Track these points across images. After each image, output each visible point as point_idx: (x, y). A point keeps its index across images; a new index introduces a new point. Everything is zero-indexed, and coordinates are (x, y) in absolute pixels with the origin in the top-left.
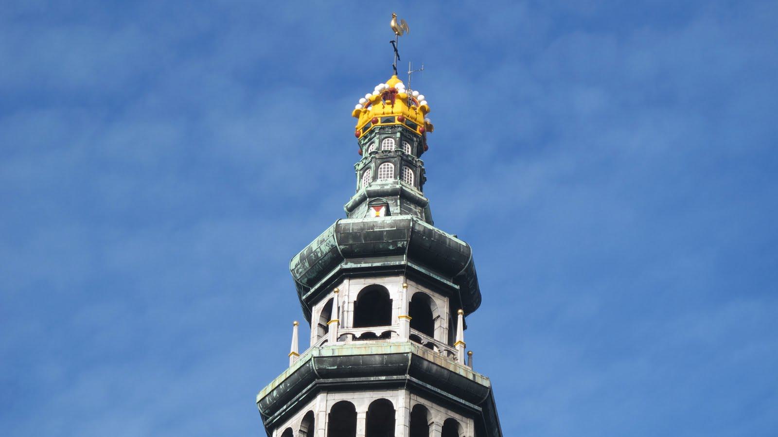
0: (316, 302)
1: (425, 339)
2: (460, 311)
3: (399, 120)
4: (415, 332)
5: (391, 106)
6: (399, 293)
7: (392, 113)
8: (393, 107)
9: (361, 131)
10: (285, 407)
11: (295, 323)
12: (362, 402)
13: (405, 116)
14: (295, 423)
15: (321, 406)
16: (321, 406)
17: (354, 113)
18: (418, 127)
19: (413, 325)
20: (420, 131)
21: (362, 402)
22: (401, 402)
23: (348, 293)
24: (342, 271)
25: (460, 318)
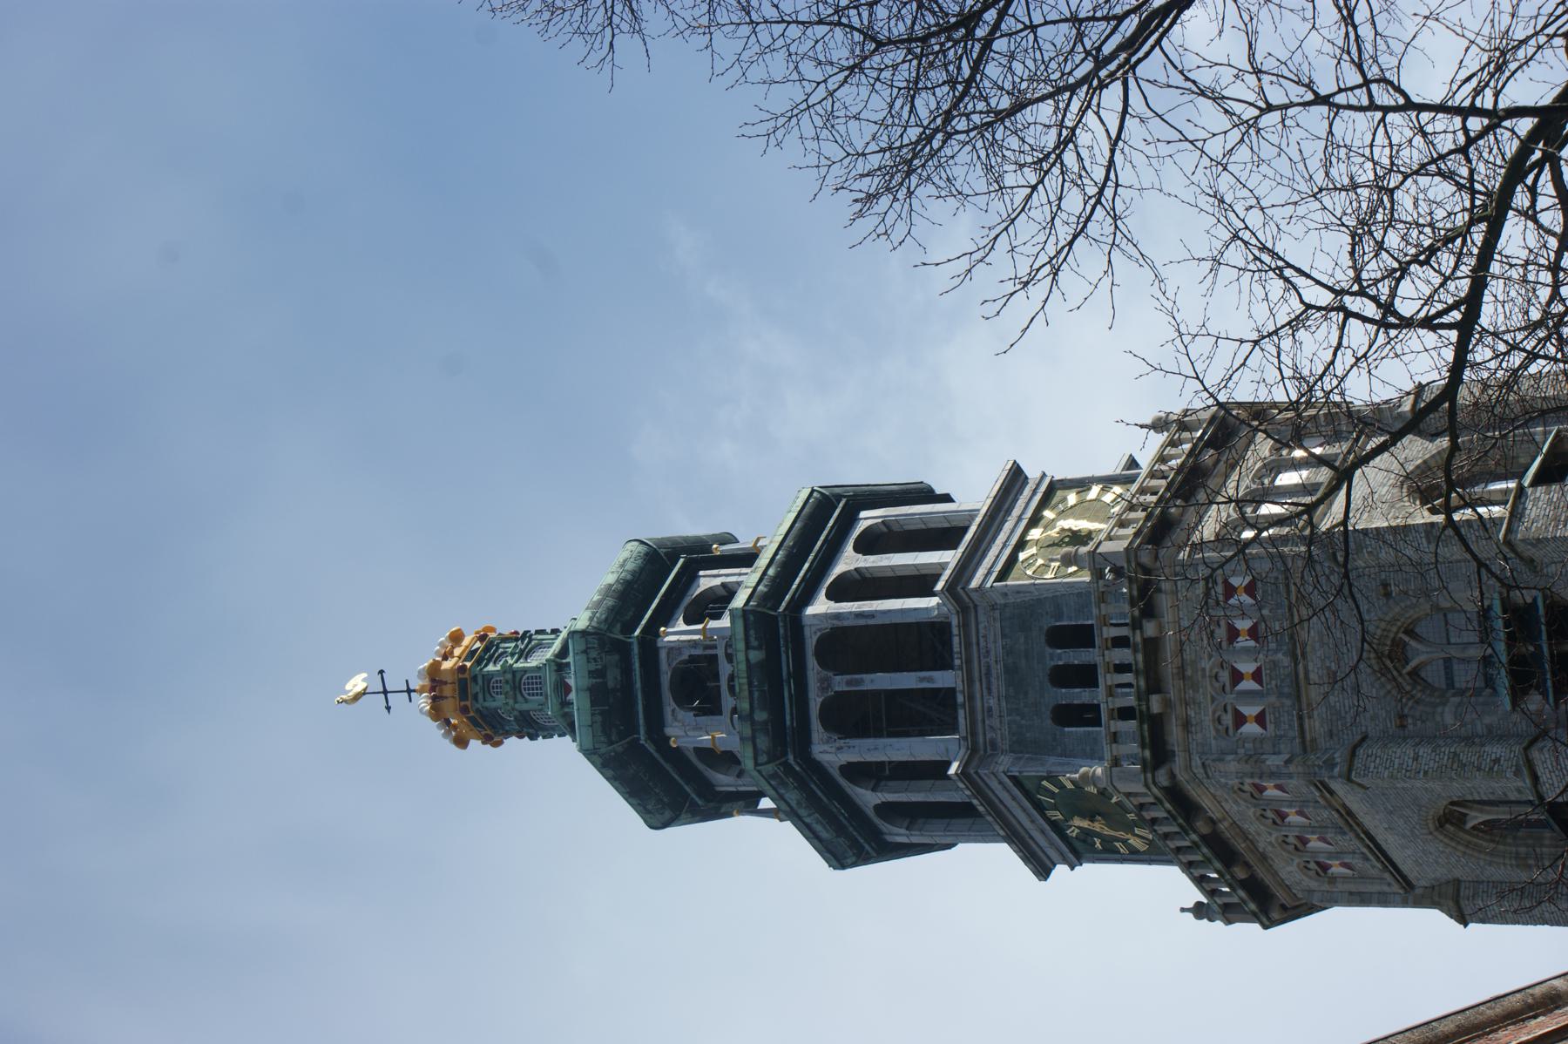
15: (830, 752)
16: (830, 752)
21: (820, 685)
24: (650, 736)
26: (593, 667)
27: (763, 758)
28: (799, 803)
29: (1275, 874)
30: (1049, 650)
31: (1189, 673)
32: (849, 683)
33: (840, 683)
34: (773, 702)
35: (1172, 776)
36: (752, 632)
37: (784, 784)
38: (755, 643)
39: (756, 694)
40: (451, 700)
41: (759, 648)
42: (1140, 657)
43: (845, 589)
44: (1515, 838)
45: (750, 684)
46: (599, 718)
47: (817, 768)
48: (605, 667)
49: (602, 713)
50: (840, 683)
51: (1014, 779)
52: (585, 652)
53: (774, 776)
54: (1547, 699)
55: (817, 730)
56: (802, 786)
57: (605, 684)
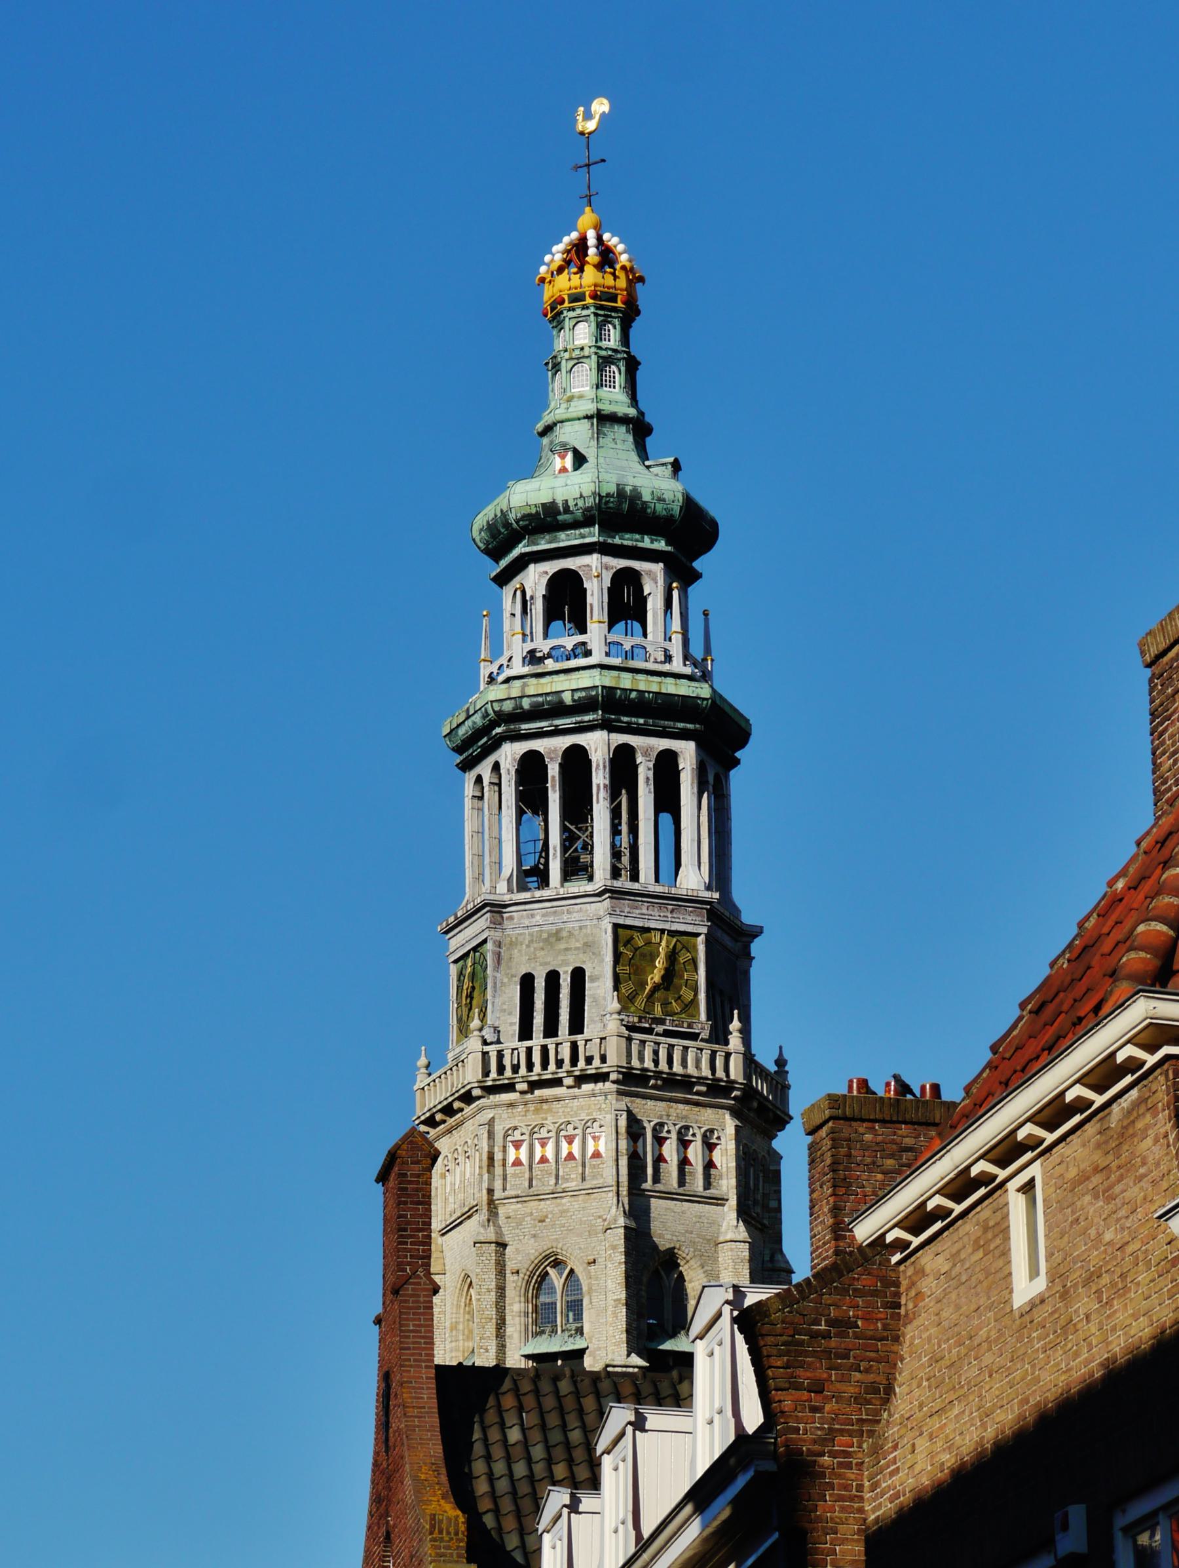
3: (592, 297)
6: (596, 574)
7: (581, 286)
8: (581, 278)
12: (552, 747)
14: (484, 769)
15: (509, 754)
16: (509, 754)
18: (619, 297)
20: (623, 303)
21: (552, 747)
22: (598, 745)
23: (536, 579)
24: (522, 555)
25: (675, 594)
26: (571, 503)
27: (497, 707)
28: (474, 723)
29: (444, 1134)
30: (570, 969)
31: (545, 1106)
33: (553, 770)
34: (537, 713)
35: (479, 1098)
36: (583, 694)
38: (576, 698)
39: (540, 699)
41: (574, 701)
42: (550, 1076)
43: (623, 765)
45: (547, 694)
46: (534, 511)
48: (572, 513)
49: (537, 513)
50: (553, 770)
51: (485, 941)
52: (581, 496)
53: (488, 715)
55: (522, 747)
56: (484, 730)
57: (559, 513)
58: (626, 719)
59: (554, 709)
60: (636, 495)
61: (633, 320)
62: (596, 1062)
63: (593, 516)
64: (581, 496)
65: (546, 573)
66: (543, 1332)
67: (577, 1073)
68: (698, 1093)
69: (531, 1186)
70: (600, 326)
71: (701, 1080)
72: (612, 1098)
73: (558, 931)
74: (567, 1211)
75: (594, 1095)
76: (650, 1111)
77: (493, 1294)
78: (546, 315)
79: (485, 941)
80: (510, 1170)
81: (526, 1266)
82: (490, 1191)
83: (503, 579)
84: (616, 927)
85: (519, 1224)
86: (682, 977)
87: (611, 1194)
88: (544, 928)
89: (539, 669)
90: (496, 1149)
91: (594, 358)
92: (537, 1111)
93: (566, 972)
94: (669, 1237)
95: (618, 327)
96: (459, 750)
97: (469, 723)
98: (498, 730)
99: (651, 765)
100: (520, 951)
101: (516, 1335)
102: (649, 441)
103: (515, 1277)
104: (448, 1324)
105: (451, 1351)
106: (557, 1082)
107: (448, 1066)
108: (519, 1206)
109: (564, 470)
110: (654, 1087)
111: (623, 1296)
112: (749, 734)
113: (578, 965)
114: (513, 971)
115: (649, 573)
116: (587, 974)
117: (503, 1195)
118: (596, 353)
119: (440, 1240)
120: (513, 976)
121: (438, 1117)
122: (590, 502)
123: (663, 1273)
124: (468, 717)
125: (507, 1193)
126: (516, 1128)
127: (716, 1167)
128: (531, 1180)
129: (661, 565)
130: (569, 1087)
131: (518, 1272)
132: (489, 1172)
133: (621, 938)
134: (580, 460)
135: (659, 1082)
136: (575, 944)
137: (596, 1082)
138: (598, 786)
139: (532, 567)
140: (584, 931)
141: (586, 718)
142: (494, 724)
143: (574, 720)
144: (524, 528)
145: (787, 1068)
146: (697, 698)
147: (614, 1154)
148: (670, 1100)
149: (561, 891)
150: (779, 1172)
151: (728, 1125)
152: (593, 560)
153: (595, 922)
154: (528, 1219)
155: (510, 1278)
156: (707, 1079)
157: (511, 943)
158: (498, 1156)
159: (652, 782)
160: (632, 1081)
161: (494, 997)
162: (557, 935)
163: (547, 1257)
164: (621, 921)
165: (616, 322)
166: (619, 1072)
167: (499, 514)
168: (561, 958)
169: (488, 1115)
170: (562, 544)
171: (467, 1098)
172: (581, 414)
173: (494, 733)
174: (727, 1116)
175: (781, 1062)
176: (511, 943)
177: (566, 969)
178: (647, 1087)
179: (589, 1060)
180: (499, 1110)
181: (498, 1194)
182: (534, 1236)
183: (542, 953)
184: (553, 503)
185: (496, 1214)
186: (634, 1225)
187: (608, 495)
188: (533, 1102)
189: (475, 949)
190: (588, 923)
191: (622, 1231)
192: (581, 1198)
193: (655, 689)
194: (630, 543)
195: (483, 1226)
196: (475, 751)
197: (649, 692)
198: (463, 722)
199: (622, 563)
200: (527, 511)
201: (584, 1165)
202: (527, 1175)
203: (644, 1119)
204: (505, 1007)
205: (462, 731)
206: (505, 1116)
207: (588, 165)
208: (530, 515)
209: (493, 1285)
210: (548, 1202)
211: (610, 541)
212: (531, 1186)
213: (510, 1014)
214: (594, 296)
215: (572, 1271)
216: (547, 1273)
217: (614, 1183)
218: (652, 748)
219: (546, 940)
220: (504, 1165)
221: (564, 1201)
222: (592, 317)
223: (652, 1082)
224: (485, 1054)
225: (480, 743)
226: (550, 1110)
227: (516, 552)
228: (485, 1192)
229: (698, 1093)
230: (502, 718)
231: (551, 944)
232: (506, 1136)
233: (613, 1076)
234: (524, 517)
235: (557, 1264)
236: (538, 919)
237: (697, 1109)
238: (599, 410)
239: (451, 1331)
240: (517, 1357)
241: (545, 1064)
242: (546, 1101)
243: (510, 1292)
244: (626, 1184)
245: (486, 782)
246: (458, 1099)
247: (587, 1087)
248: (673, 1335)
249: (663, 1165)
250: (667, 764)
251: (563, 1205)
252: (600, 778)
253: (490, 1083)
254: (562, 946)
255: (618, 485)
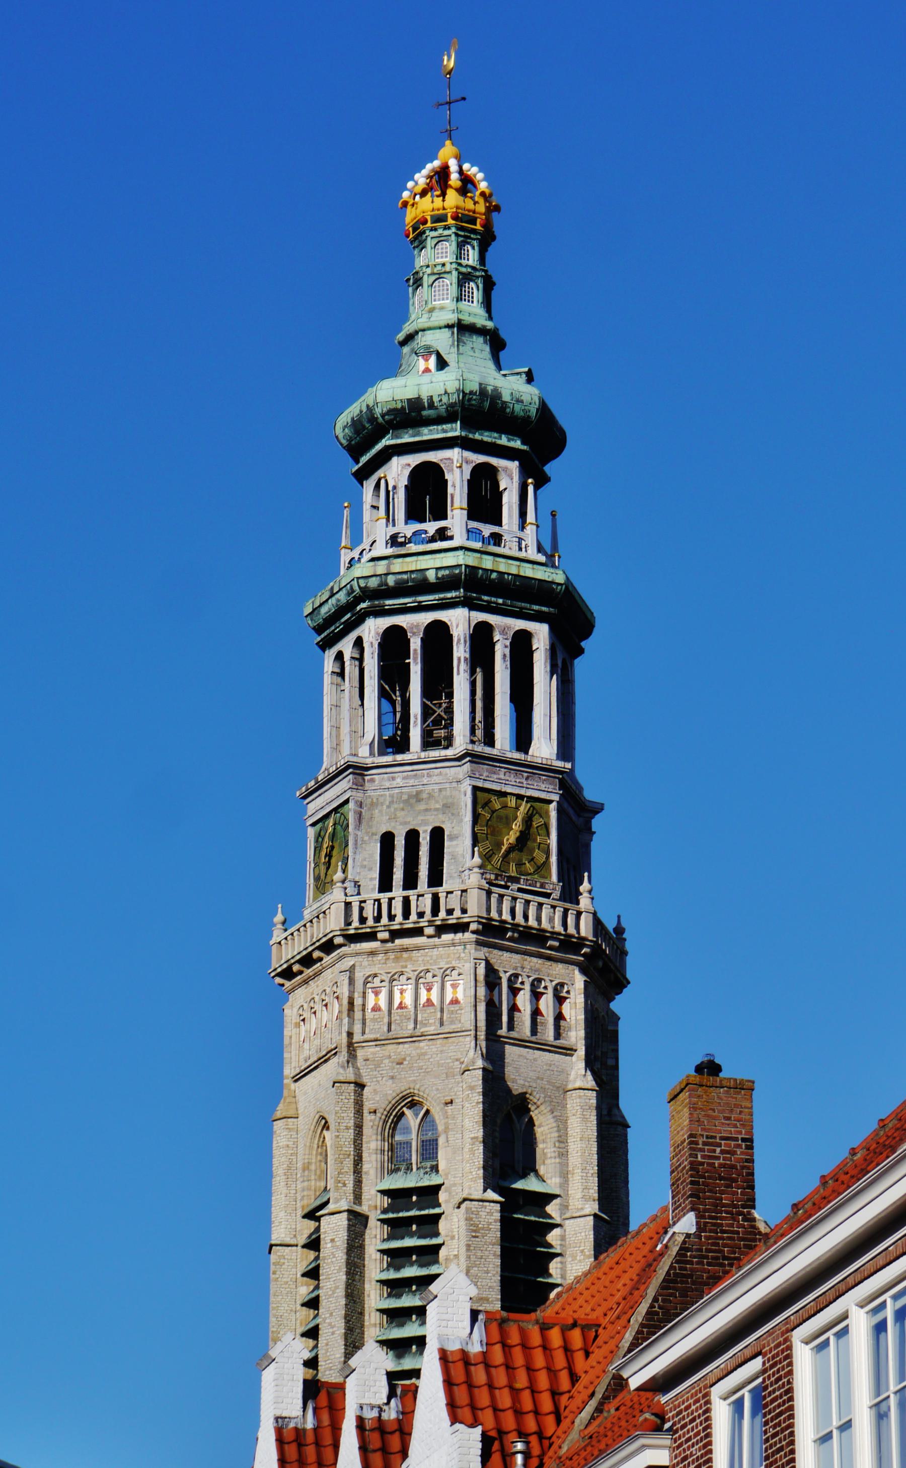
0: (367, 477)
1: (487, 530)
2: (530, 481)
3: (453, 218)
4: (473, 524)
5: (441, 198)
6: (457, 467)
7: (444, 209)
8: (444, 201)
9: (411, 229)
10: (333, 628)
11: (346, 505)
12: (415, 623)
13: (460, 211)
14: (346, 646)
15: (372, 630)
16: (372, 630)
17: (400, 204)
18: (478, 221)
19: (471, 517)
20: (482, 226)
21: (415, 623)
22: (459, 621)
23: (398, 471)
24: (387, 448)
25: (531, 489)
26: (436, 399)
27: (362, 583)
28: (338, 600)
29: (300, 985)
30: (429, 828)
31: (405, 955)
32: (415, 650)
33: (415, 644)
34: (401, 590)
35: (340, 946)
36: (447, 572)
37: (349, 594)
38: (440, 575)
39: (405, 577)
40: (430, 207)
41: (437, 578)
42: (411, 926)
43: (481, 638)
44: (320, 1161)
45: (412, 572)
46: (399, 406)
47: (360, 620)
49: (403, 408)
50: (415, 644)
51: (347, 802)
52: (446, 392)
53: (352, 591)
54: (384, 1211)
55: (385, 622)
57: (424, 408)
58: (486, 598)
59: (418, 586)
60: (496, 396)
61: (489, 245)
62: (457, 913)
63: (456, 413)
64: (446, 392)
65: (409, 465)
66: (397, 1170)
67: (439, 923)
68: (551, 948)
69: (389, 1030)
70: (460, 246)
71: (554, 935)
72: (471, 948)
73: (418, 793)
74: (425, 1054)
75: (454, 945)
76: (507, 962)
77: (352, 1131)
78: (408, 236)
79: (347, 802)
80: (369, 1014)
81: (384, 1106)
82: (350, 1035)
83: (362, 475)
84: (475, 789)
85: (377, 1066)
86: (535, 840)
87: (468, 1039)
88: (404, 790)
89: (403, 551)
90: (356, 995)
91: (455, 273)
92: (397, 959)
93: (425, 831)
94: (522, 1082)
95: (477, 248)
96: (319, 630)
97: (333, 601)
98: (363, 605)
99: (508, 643)
100: (381, 811)
101: (372, 1172)
102: (502, 355)
103: (373, 1117)
104: (300, 1165)
105: (303, 1190)
106: (417, 932)
107: (302, 923)
108: (378, 1049)
109: (427, 370)
110: (511, 939)
111: (480, 1134)
112: (593, 626)
113: (437, 824)
114: (374, 830)
115: (506, 469)
116: (446, 833)
117: (362, 1038)
118: (457, 269)
119: (293, 1086)
120: (373, 834)
121: (296, 968)
122: (454, 399)
123: (514, 1117)
124: (332, 595)
125: (368, 1036)
126: (375, 976)
127: (565, 1019)
128: (390, 1024)
129: (517, 463)
130: (429, 937)
131: (375, 1112)
132: (349, 1016)
133: (479, 800)
134: (442, 364)
135: (516, 935)
136: (433, 805)
137: (455, 932)
138: (459, 659)
139: (395, 460)
140: (444, 793)
141: (449, 595)
142: (358, 600)
143: (437, 597)
144: (389, 423)
145: (624, 936)
146: (553, 582)
147: (473, 1000)
148: (525, 953)
149: (423, 755)
150: (617, 1031)
151: (578, 981)
152: (455, 454)
153: (455, 785)
154: (386, 1061)
155: (368, 1118)
156: (560, 934)
157: (372, 804)
158: (358, 1001)
159: (508, 658)
160: (491, 932)
161: (355, 853)
162: (417, 797)
163: (404, 1098)
164: (480, 784)
165: (475, 243)
166: (479, 923)
167: (365, 410)
168: (420, 818)
169: (348, 963)
170: (425, 438)
171: (328, 947)
172: (443, 323)
173: (358, 608)
174: (577, 972)
175: (619, 930)
176: (372, 804)
177: (426, 828)
178: (504, 939)
179: (450, 912)
180: (360, 958)
181: (357, 1037)
182: (392, 1078)
183: (403, 813)
184: (419, 399)
185: (355, 1057)
186: (490, 1067)
187: (471, 393)
188: (393, 950)
189: (335, 810)
190: (447, 785)
191: (480, 1072)
192: (439, 1042)
193: (514, 571)
194: (489, 440)
195: (343, 1067)
196: (337, 627)
197: (509, 574)
198: (327, 601)
199: (481, 459)
200: (393, 405)
201: (442, 1010)
202: (386, 1020)
203: (501, 969)
204: (365, 863)
205: (324, 610)
206: (365, 963)
207: (450, 103)
208: (395, 410)
209: (351, 1123)
210: (406, 1046)
211: (471, 436)
212: (389, 1030)
213: (370, 869)
214: (455, 217)
215: (428, 1112)
216: (403, 1114)
217: (473, 1028)
218: (509, 628)
219: (406, 802)
220: (363, 1010)
221: (422, 1044)
222: (453, 237)
223: (509, 934)
224: (348, 905)
225: (343, 620)
226: (410, 959)
227: (379, 446)
228: (344, 1035)
229: (551, 948)
230: (367, 594)
231: (412, 806)
232: (366, 983)
233: (473, 927)
234: (390, 412)
235: (413, 1105)
236: (399, 781)
237: (549, 963)
238: (459, 320)
239: (304, 1170)
240: (373, 1192)
241: (406, 914)
242: (406, 950)
243: (367, 1131)
244: (484, 1028)
245: (347, 657)
246: (318, 948)
247: (447, 937)
248: (524, 1176)
249: (517, 1014)
250: (521, 645)
251: (422, 1048)
252: (460, 652)
253: (352, 932)
254: (422, 806)
255: (480, 384)
